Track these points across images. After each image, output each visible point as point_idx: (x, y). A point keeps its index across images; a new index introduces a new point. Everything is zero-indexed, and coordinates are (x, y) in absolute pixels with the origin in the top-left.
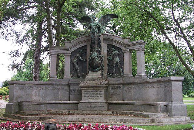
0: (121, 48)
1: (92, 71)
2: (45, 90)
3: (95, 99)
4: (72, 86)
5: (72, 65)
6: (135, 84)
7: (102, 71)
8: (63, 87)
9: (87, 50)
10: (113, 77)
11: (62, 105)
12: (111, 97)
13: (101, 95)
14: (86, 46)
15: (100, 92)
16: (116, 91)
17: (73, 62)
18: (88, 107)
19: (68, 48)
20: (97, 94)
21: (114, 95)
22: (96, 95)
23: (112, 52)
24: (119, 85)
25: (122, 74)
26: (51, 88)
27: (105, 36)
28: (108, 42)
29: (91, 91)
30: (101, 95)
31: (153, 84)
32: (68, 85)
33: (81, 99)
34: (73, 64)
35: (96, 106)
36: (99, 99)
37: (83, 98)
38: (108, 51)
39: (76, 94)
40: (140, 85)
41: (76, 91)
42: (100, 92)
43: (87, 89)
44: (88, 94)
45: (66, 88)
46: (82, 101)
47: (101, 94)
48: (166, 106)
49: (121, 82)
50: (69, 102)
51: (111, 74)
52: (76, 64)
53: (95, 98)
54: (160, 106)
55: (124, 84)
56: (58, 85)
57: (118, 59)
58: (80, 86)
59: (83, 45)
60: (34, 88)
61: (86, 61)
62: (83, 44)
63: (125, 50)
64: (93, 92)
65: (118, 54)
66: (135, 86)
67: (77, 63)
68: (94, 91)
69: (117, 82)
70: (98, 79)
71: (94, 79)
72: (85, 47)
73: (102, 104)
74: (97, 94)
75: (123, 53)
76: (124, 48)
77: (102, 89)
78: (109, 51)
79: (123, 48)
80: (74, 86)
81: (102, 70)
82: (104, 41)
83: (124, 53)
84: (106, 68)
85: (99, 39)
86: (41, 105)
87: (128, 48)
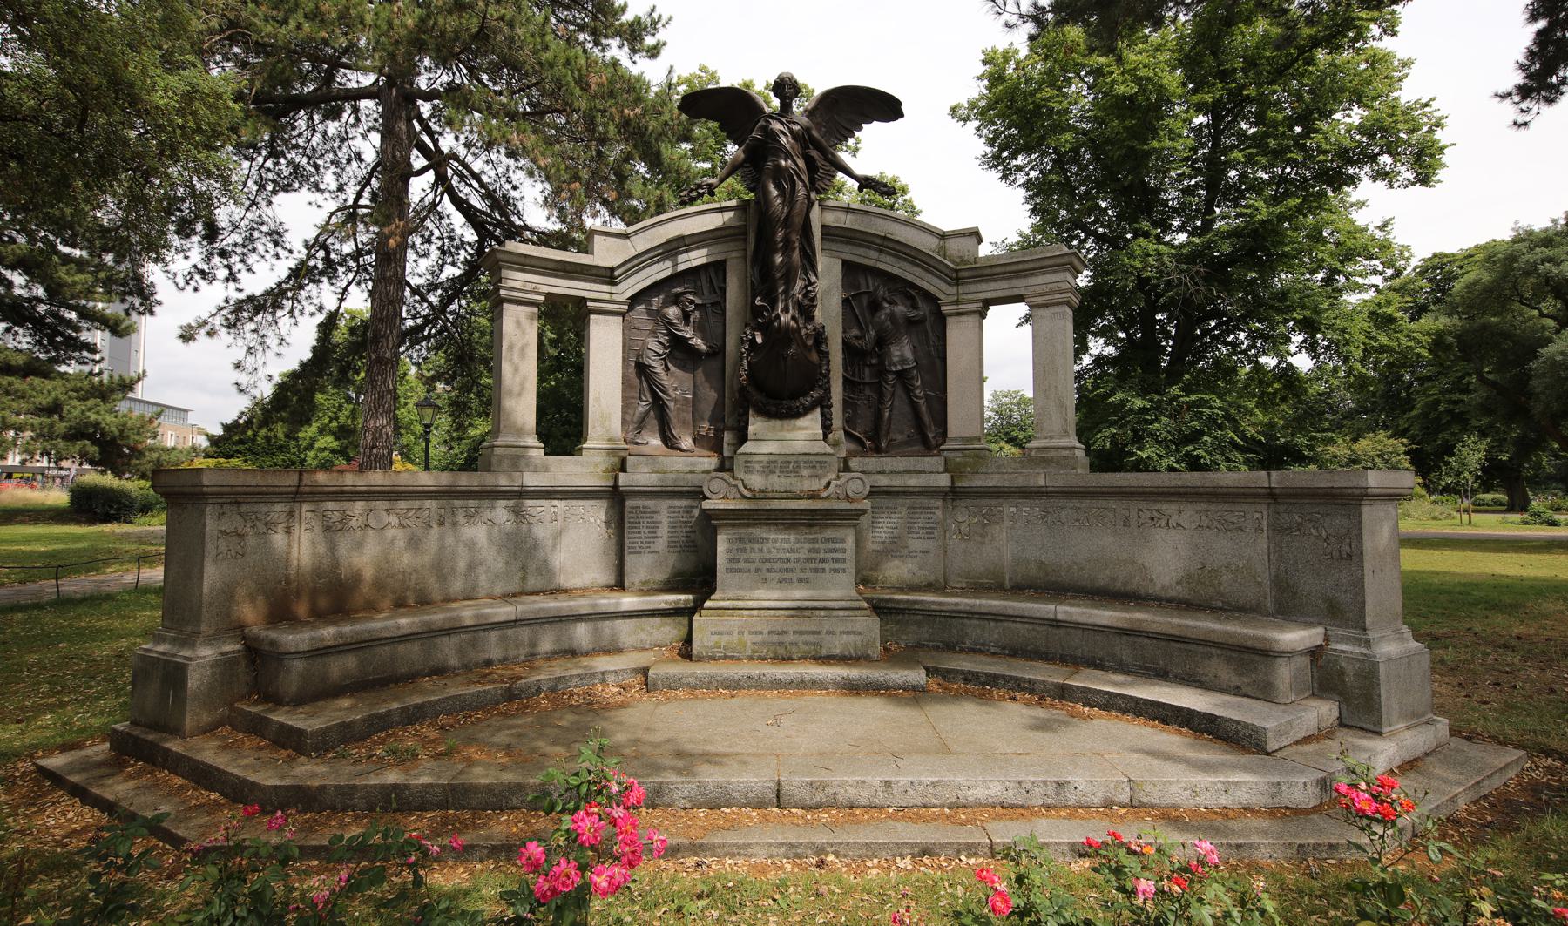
0: (932, 290)
1: (767, 414)
5: (639, 371)
6: (1026, 493)
7: (823, 415)
8: (580, 506)
9: (723, 290)
13: (837, 561)
15: (833, 541)
17: (639, 356)
19: (612, 270)
23: (875, 307)
24: (924, 501)
25: (931, 435)
28: (848, 248)
30: (837, 561)
31: (1170, 508)
38: (846, 301)
40: (1063, 502)
43: (748, 525)
48: (1315, 653)
49: (943, 481)
50: (628, 602)
51: (870, 437)
52: (657, 366)
53: (800, 581)
54: (1290, 654)
55: (953, 494)
57: (909, 354)
58: (706, 505)
59: (698, 257)
61: (717, 352)
62: (704, 251)
63: (957, 303)
65: (911, 323)
66: (1027, 509)
67: (666, 360)
71: (787, 464)
75: (941, 320)
76: (954, 290)
77: (842, 525)
78: (859, 305)
79: (943, 286)
82: (827, 244)
83: (949, 320)
87: (972, 288)
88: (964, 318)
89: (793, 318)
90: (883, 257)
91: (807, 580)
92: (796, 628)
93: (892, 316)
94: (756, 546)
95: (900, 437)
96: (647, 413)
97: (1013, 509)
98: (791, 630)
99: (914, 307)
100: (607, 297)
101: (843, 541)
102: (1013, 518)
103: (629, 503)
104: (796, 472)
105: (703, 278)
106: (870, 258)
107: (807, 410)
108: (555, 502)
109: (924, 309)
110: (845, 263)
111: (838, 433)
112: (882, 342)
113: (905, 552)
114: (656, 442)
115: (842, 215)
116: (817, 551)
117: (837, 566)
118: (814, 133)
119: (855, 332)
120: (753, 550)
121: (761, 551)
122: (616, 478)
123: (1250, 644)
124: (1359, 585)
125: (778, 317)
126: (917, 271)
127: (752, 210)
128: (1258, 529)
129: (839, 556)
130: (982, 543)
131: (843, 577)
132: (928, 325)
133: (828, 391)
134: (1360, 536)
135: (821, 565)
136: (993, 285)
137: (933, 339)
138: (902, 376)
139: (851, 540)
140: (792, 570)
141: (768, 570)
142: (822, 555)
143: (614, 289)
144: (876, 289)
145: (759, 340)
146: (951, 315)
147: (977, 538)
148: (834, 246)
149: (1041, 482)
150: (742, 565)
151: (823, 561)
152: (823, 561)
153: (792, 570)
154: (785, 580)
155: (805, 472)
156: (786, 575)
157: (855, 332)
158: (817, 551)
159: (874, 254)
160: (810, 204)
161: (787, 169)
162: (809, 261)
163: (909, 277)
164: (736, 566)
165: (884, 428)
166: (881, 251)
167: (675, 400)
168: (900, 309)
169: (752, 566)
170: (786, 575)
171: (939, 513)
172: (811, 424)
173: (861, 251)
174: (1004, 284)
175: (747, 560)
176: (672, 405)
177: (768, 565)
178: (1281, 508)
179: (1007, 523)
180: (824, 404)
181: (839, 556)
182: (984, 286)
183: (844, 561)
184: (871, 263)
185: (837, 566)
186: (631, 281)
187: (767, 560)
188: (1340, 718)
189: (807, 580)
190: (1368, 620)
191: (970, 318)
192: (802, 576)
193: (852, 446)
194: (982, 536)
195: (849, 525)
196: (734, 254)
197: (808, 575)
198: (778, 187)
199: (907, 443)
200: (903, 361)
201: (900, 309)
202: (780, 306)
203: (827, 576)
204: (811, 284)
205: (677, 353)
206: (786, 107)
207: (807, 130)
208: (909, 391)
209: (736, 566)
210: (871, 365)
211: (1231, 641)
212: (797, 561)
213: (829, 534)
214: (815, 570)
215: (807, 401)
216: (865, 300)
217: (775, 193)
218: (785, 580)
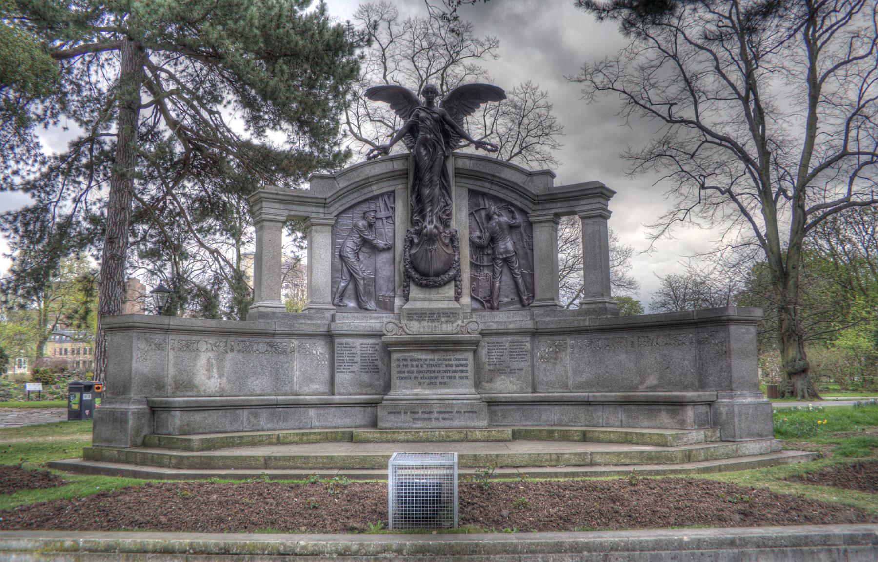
1: (420, 285)
2: (240, 356)
3: (439, 388)
4: (344, 340)
7: (456, 286)
9: (393, 209)
10: (492, 308)
11: (312, 412)
12: (490, 381)
13: (463, 371)
14: (391, 194)
15: (460, 359)
16: (506, 357)
18: (416, 416)
20: (449, 368)
21: (501, 372)
22: (445, 372)
23: (489, 218)
25: (525, 298)
26: (262, 347)
27: (460, 163)
28: (472, 182)
29: (424, 357)
30: (463, 371)
32: (330, 337)
33: (387, 388)
34: (342, 257)
35: (449, 412)
36: (456, 387)
37: (395, 382)
38: (471, 214)
39: (356, 368)
41: (358, 359)
42: (460, 359)
43: (409, 351)
44: (415, 369)
45: (319, 349)
46: (392, 395)
47: (461, 368)
49: (529, 324)
53: (441, 383)
54: (693, 403)
56: (290, 335)
57: (510, 246)
60: (203, 346)
62: (382, 185)
64: (433, 360)
65: (512, 228)
68: (436, 356)
69: (511, 326)
70: (450, 315)
72: (386, 197)
73: (472, 405)
74: (449, 368)
77: (466, 350)
79: (530, 205)
80: (350, 340)
81: (456, 281)
82: (459, 180)
83: (535, 226)
84: (466, 274)
85: (444, 173)
86: (237, 411)
88: (543, 225)
89: (435, 227)
90: (494, 187)
91: (445, 384)
92: (438, 410)
93: (500, 224)
94: (414, 363)
95: (506, 300)
96: (346, 288)
97: (573, 342)
98: (435, 411)
99: (513, 218)
100: (322, 216)
101: (466, 359)
102: (572, 347)
103: (337, 340)
104: (438, 320)
105: (381, 201)
106: (487, 188)
107: (446, 283)
108: (293, 341)
109: (519, 219)
110: (470, 190)
111: (466, 300)
112: (493, 240)
113: (508, 370)
114: (352, 304)
115: (467, 161)
116: (451, 366)
117: (463, 375)
118: (448, 117)
119: (478, 233)
120: (412, 366)
121: (417, 366)
122: (329, 326)
123: (675, 400)
124: (729, 366)
125: (426, 227)
126: (514, 195)
127: (411, 158)
128: (691, 343)
129: (465, 369)
130: (555, 364)
131: (465, 381)
132: (522, 229)
133: (459, 272)
134: (729, 341)
135: (453, 374)
136: (559, 205)
137: (526, 238)
138: (506, 260)
139: (470, 362)
140: (436, 378)
141: (422, 378)
142: (454, 368)
143: (326, 211)
144: (490, 206)
145: (416, 241)
146: (535, 223)
147: (552, 360)
148: (463, 180)
149: (587, 324)
150: (406, 375)
151: (454, 371)
152: (454, 371)
153: (436, 378)
154: (432, 383)
155: (443, 319)
156: (432, 381)
157: (478, 233)
158: (451, 366)
159: (487, 185)
160: (446, 158)
161: (430, 139)
162: (446, 188)
163: (510, 199)
164: (402, 375)
165: (496, 293)
166: (492, 183)
167: (364, 279)
168: (505, 219)
169: (412, 376)
170: (432, 381)
171: (528, 345)
172: (449, 291)
173: (480, 183)
174: (566, 204)
175: (408, 372)
176: (362, 282)
177: (422, 375)
178: (700, 330)
179: (569, 350)
180: (456, 279)
181: (465, 369)
182: (554, 205)
183: (467, 371)
184: (486, 190)
185: (463, 375)
186: (336, 205)
187: (421, 372)
188: (721, 437)
189: (445, 384)
190: (734, 386)
191: (547, 225)
192: (442, 381)
193: (476, 305)
194: (555, 359)
195: (470, 350)
196: (400, 187)
197: (446, 380)
198: (426, 148)
199: (510, 303)
200: (507, 251)
201: (505, 219)
202: (428, 219)
203: (457, 381)
204: (447, 205)
205: (364, 249)
206: (430, 103)
207: (443, 116)
208: (511, 270)
209: (402, 375)
210: (488, 255)
211: (667, 400)
212: (440, 372)
213: (458, 356)
214: (450, 377)
215: (446, 277)
216: (483, 213)
217: (424, 153)
218: (432, 383)
